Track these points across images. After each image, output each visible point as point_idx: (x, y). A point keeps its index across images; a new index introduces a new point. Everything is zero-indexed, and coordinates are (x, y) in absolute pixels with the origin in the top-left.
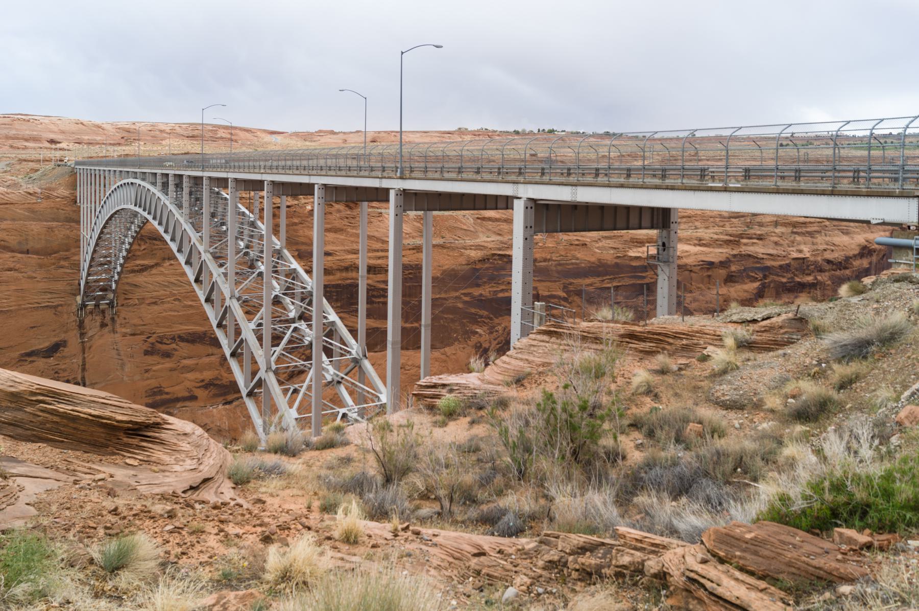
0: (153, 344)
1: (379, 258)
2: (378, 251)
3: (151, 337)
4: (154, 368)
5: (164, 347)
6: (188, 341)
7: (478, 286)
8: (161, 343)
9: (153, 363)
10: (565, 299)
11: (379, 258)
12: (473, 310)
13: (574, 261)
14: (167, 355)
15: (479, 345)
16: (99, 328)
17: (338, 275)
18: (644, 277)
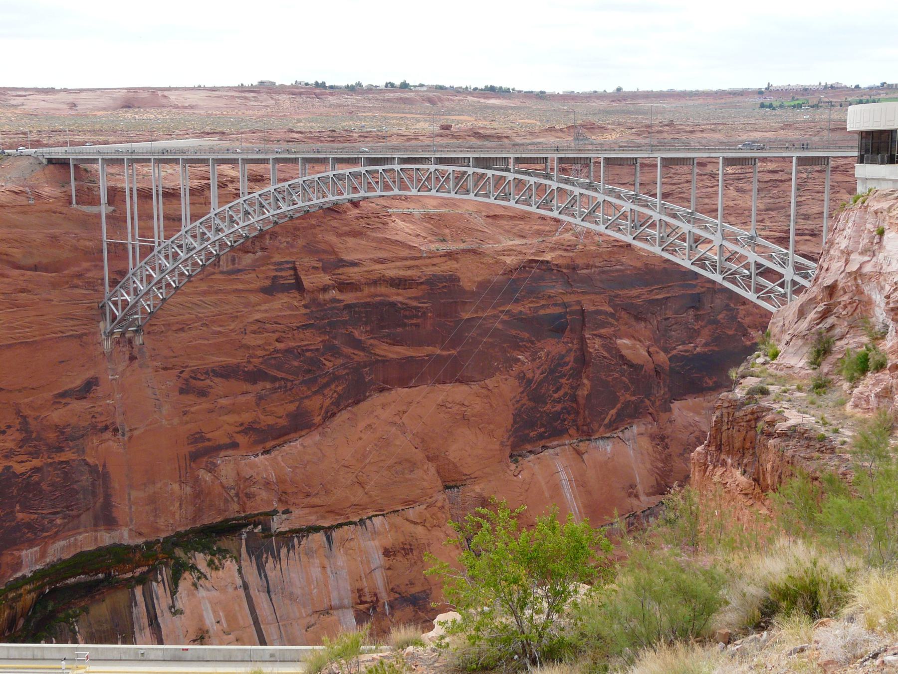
0: (186, 380)
1: (409, 268)
2: (406, 259)
3: (183, 371)
4: (193, 409)
5: (199, 384)
6: (221, 376)
7: (517, 301)
8: (195, 378)
9: (190, 403)
10: (612, 315)
11: (409, 268)
12: (513, 332)
13: (618, 267)
14: (203, 393)
15: (522, 375)
16: (128, 362)
17: (367, 290)
18: (695, 286)
